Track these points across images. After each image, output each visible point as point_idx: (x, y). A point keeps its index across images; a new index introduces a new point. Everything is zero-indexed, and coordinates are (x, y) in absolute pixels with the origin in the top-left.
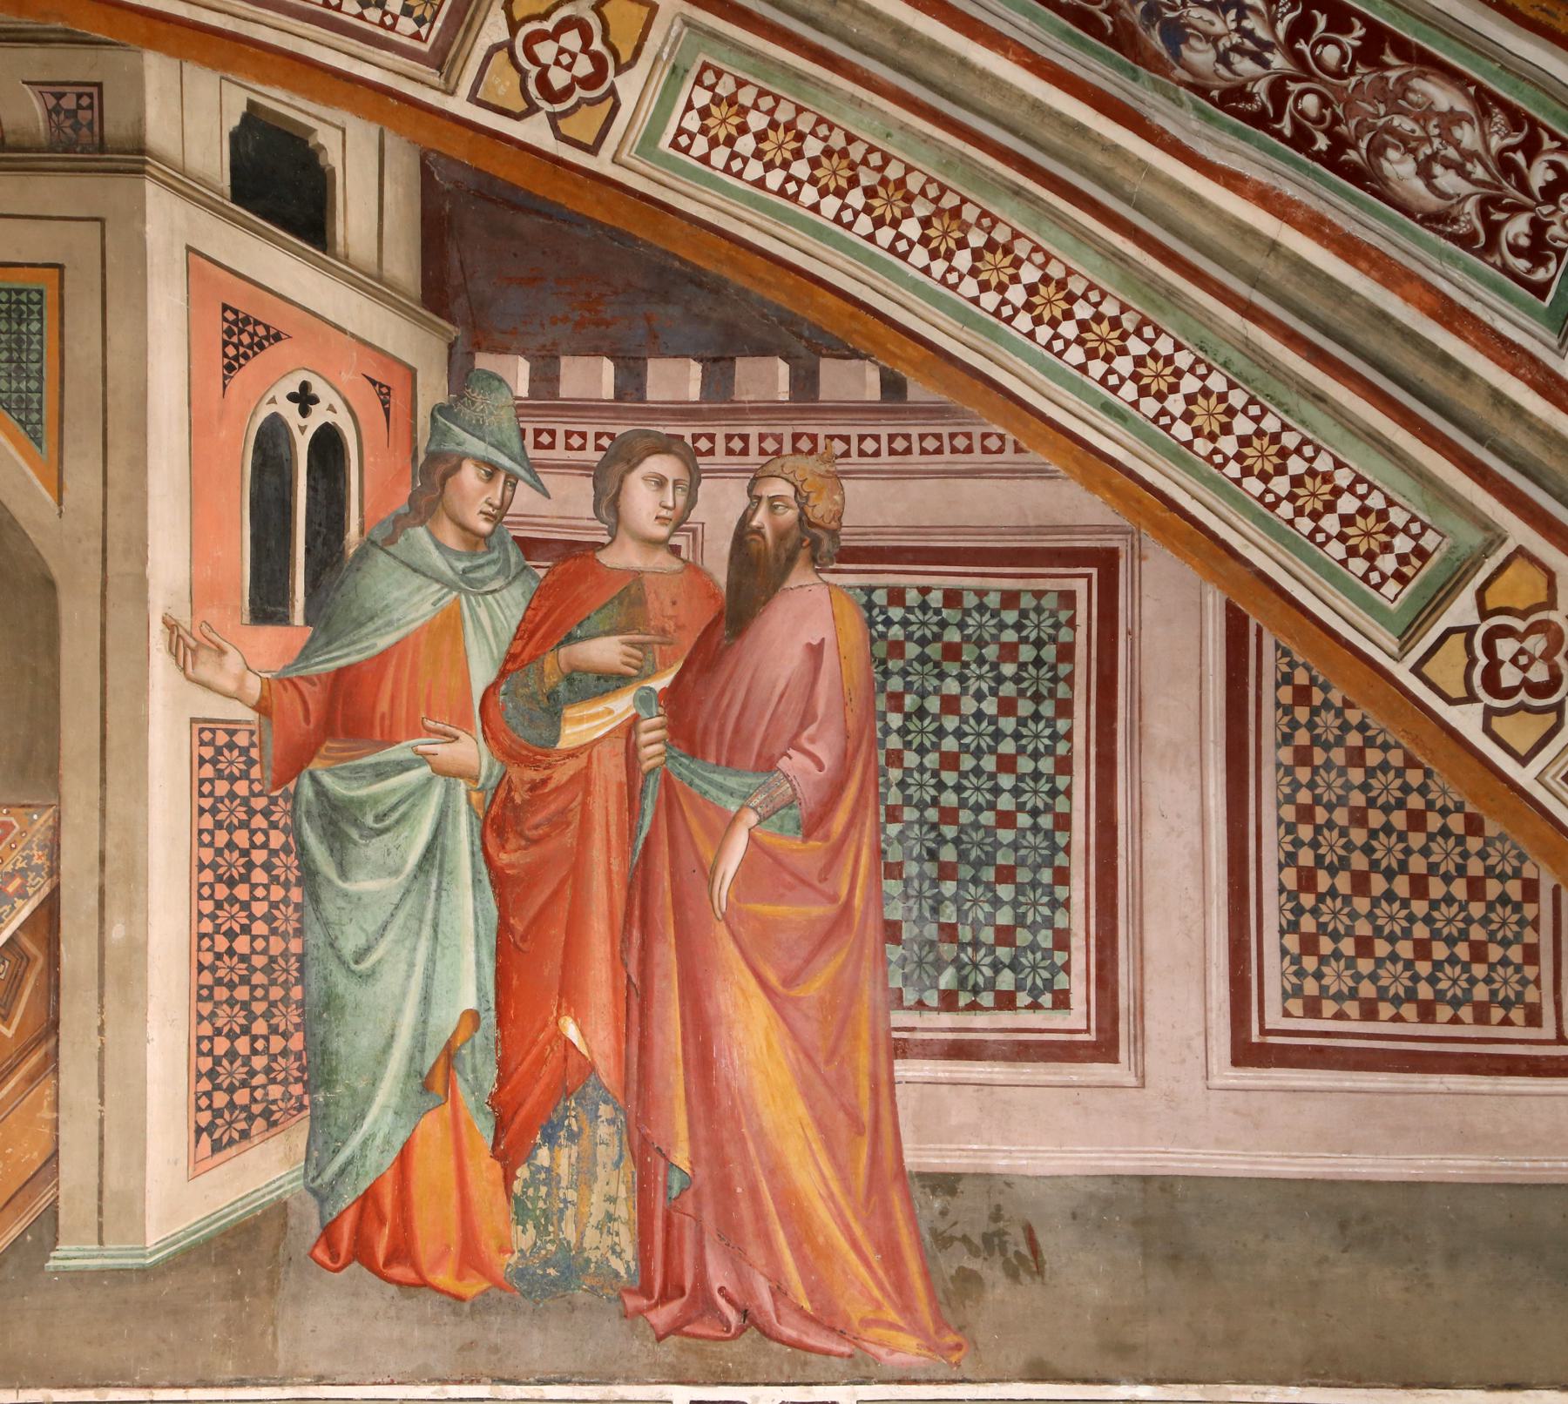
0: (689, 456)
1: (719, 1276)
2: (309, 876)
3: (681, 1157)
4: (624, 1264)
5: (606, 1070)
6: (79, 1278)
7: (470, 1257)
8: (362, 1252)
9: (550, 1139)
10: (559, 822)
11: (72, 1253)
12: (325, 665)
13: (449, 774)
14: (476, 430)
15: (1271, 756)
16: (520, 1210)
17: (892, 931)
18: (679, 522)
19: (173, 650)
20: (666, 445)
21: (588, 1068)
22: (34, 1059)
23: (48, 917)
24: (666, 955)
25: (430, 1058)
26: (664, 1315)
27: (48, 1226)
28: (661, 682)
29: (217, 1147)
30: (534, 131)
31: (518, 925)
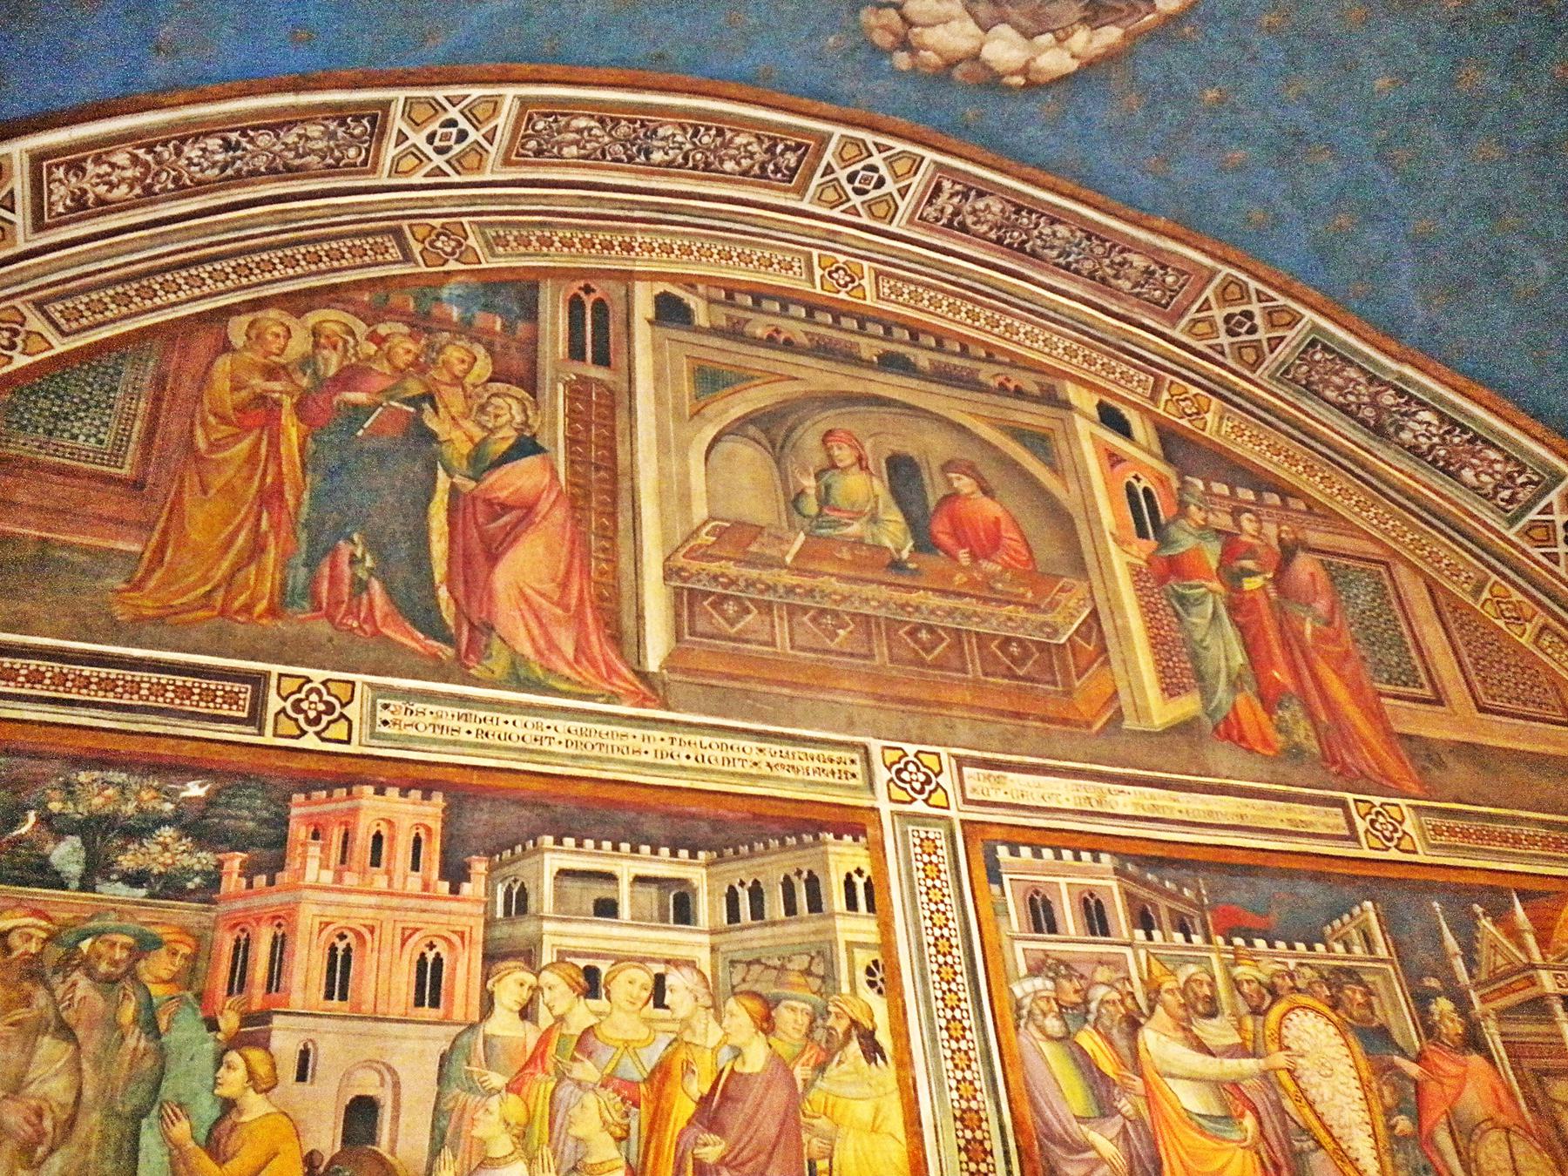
0: (1257, 515)
1: (1349, 760)
2: (1177, 614)
3: (1324, 718)
4: (1316, 750)
5: (1292, 688)
6: (1134, 733)
7: (1266, 743)
8: (1229, 736)
9: (1280, 706)
10: (1250, 612)
11: (1129, 724)
12: (1166, 553)
13: (1214, 592)
14: (1193, 496)
15: (1453, 626)
16: (1280, 731)
17: (1364, 658)
18: (1259, 531)
19: (1115, 540)
20: (1249, 511)
21: (1285, 686)
22: (1101, 659)
23: (1094, 613)
24: (1298, 654)
25: (1234, 677)
26: (1334, 769)
27: (1119, 714)
28: (1270, 575)
29: (1171, 696)
30: (1184, 422)
31: (1249, 640)
